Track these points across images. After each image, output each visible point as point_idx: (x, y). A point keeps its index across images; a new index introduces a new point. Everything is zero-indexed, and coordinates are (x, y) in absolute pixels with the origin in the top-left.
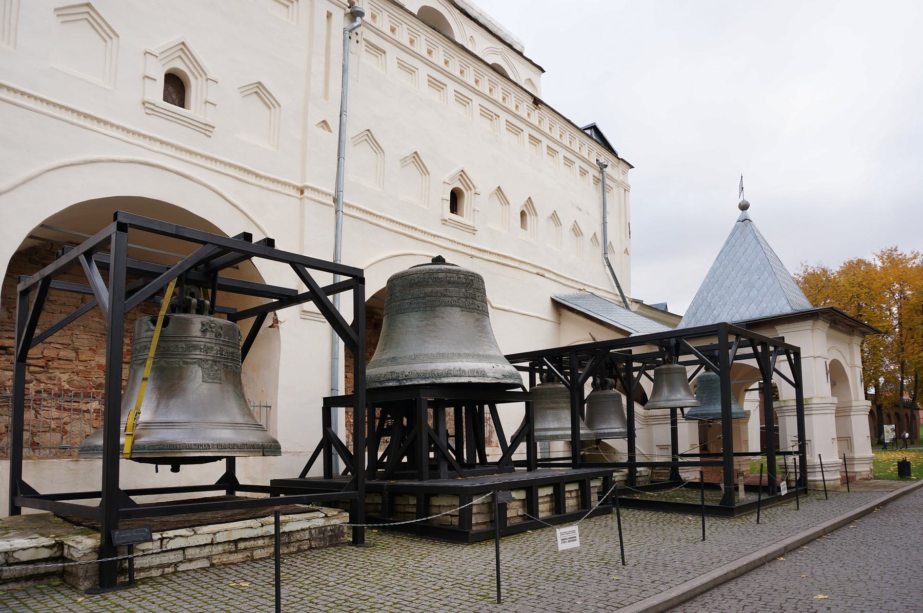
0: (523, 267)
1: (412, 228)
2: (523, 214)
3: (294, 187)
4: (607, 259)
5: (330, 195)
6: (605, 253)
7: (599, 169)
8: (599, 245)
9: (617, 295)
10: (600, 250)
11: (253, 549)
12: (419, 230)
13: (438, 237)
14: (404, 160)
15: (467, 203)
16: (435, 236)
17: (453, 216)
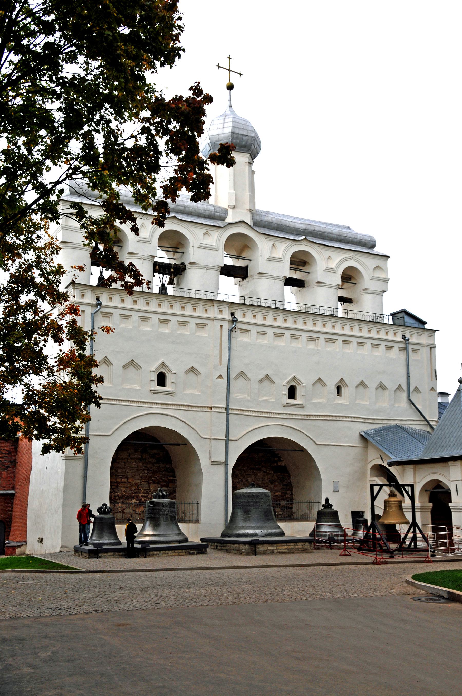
0: (338, 419)
1: (266, 412)
2: (339, 389)
3: (208, 407)
4: (410, 400)
5: (223, 408)
6: (409, 396)
7: (404, 342)
8: (404, 391)
9: (422, 421)
10: (405, 395)
11: (179, 553)
12: (270, 413)
13: (281, 414)
14: (261, 381)
15: (299, 392)
16: (279, 414)
17: (292, 401)
